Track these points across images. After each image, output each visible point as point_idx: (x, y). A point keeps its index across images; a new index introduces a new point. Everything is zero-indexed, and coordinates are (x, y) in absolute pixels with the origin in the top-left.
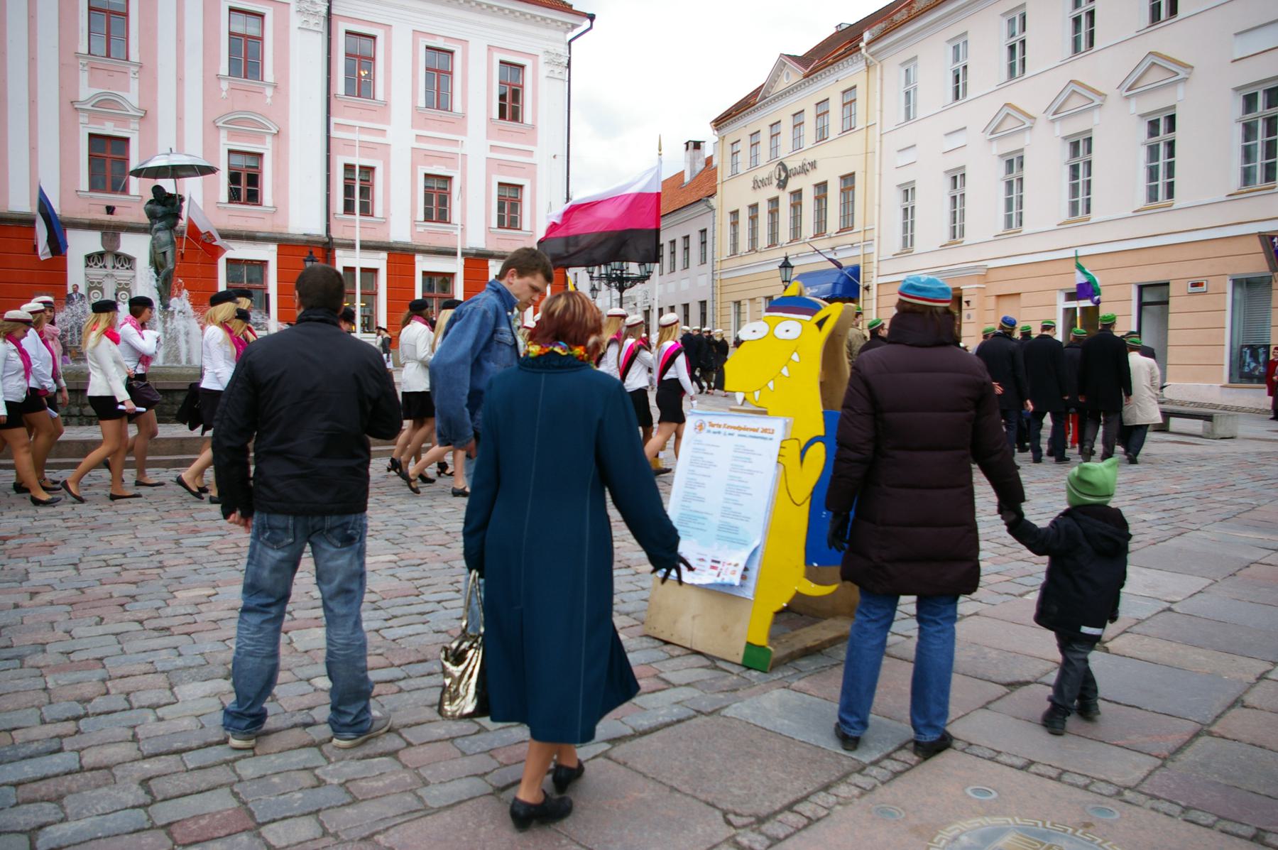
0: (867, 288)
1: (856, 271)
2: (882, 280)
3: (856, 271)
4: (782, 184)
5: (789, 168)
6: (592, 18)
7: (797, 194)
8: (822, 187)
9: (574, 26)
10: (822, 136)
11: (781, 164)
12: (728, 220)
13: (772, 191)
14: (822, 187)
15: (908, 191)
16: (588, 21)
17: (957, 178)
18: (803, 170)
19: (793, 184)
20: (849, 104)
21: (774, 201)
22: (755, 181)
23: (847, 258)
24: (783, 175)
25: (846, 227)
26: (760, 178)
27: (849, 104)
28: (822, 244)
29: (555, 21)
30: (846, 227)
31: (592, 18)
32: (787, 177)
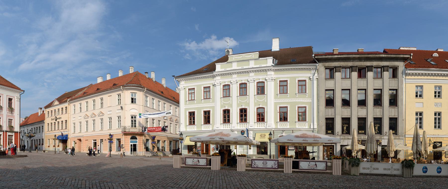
0: (69, 138)
1: (67, 135)
2: (71, 137)
3: (67, 135)
4: (56, 120)
5: (57, 118)
6: (24, 91)
7: (59, 122)
8: (62, 121)
9: (21, 92)
10: (62, 114)
11: (56, 117)
12: (47, 125)
13: (54, 121)
14: (62, 121)
15: (74, 124)
16: (23, 92)
17: (80, 123)
18: (59, 118)
19: (58, 120)
20: (66, 109)
21: (55, 123)
22: (52, 119)
23: (65, 134)
24: (56, 119)
25: (66, 128)
26: (52, 118)
27: (66, 109)
28: (62, 131)
29: (18, 91)
30: (66, 128)
31: (24, 91)
32: (57, 119)
